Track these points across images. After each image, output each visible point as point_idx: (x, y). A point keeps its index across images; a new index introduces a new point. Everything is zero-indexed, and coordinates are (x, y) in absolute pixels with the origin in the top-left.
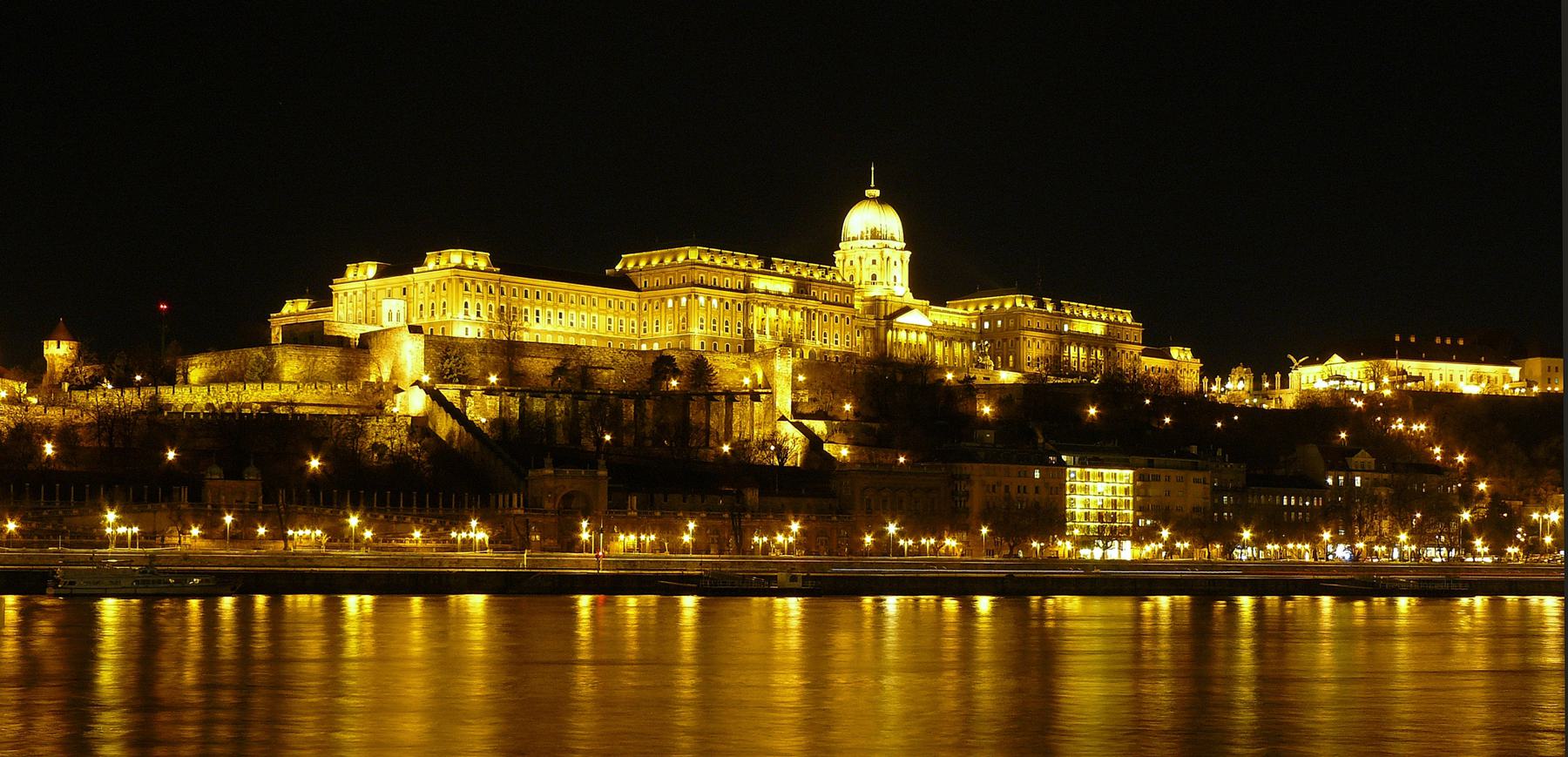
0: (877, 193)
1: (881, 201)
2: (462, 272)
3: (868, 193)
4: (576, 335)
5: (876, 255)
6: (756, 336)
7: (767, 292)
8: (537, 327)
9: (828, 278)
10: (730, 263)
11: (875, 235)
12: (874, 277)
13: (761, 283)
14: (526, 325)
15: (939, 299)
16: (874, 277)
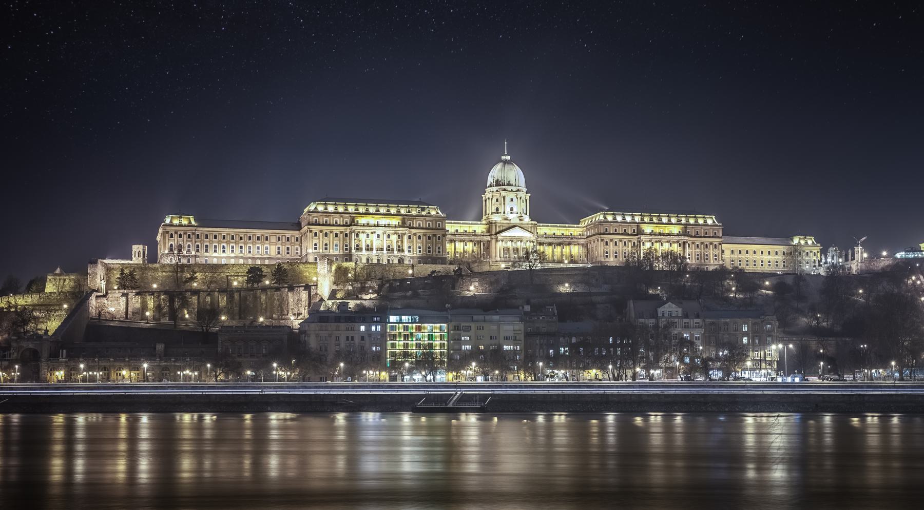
0: (508, 158)
1: (506, 162)
2: (168, 228)
3: (503, 157)
4: (253, 258)
5: (497, 196)
6: (353, 251)
8: (224, 255)
9: (423, 213)
10: (341, 209)
11: (498, 183)
12: (497, 209)
13: (362, 220)
14: (215, 254)
15: (575, 220)
16: (497, 209)
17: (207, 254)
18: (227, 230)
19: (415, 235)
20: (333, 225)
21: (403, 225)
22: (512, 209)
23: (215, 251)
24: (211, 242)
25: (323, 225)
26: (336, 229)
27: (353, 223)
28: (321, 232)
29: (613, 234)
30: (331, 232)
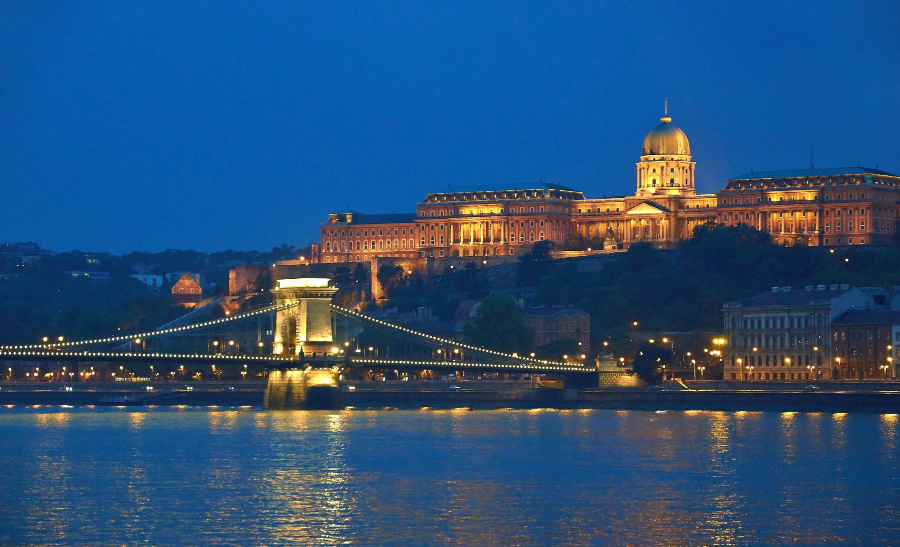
6: (451, 244)
7: (472, 215)
13: (466, 211)
17: (359, 252)
18: (375, 225)
19: (517, 222)
20: (439, 218)
21: (506, 213)
22: (654, 181)
23: (366, 248)
24: (362, 239)
25: (430, 218)
26: (441, 222)
27: (458, 215)
28: (428, 225)
29: (733, 206)
30: (437, 225)
